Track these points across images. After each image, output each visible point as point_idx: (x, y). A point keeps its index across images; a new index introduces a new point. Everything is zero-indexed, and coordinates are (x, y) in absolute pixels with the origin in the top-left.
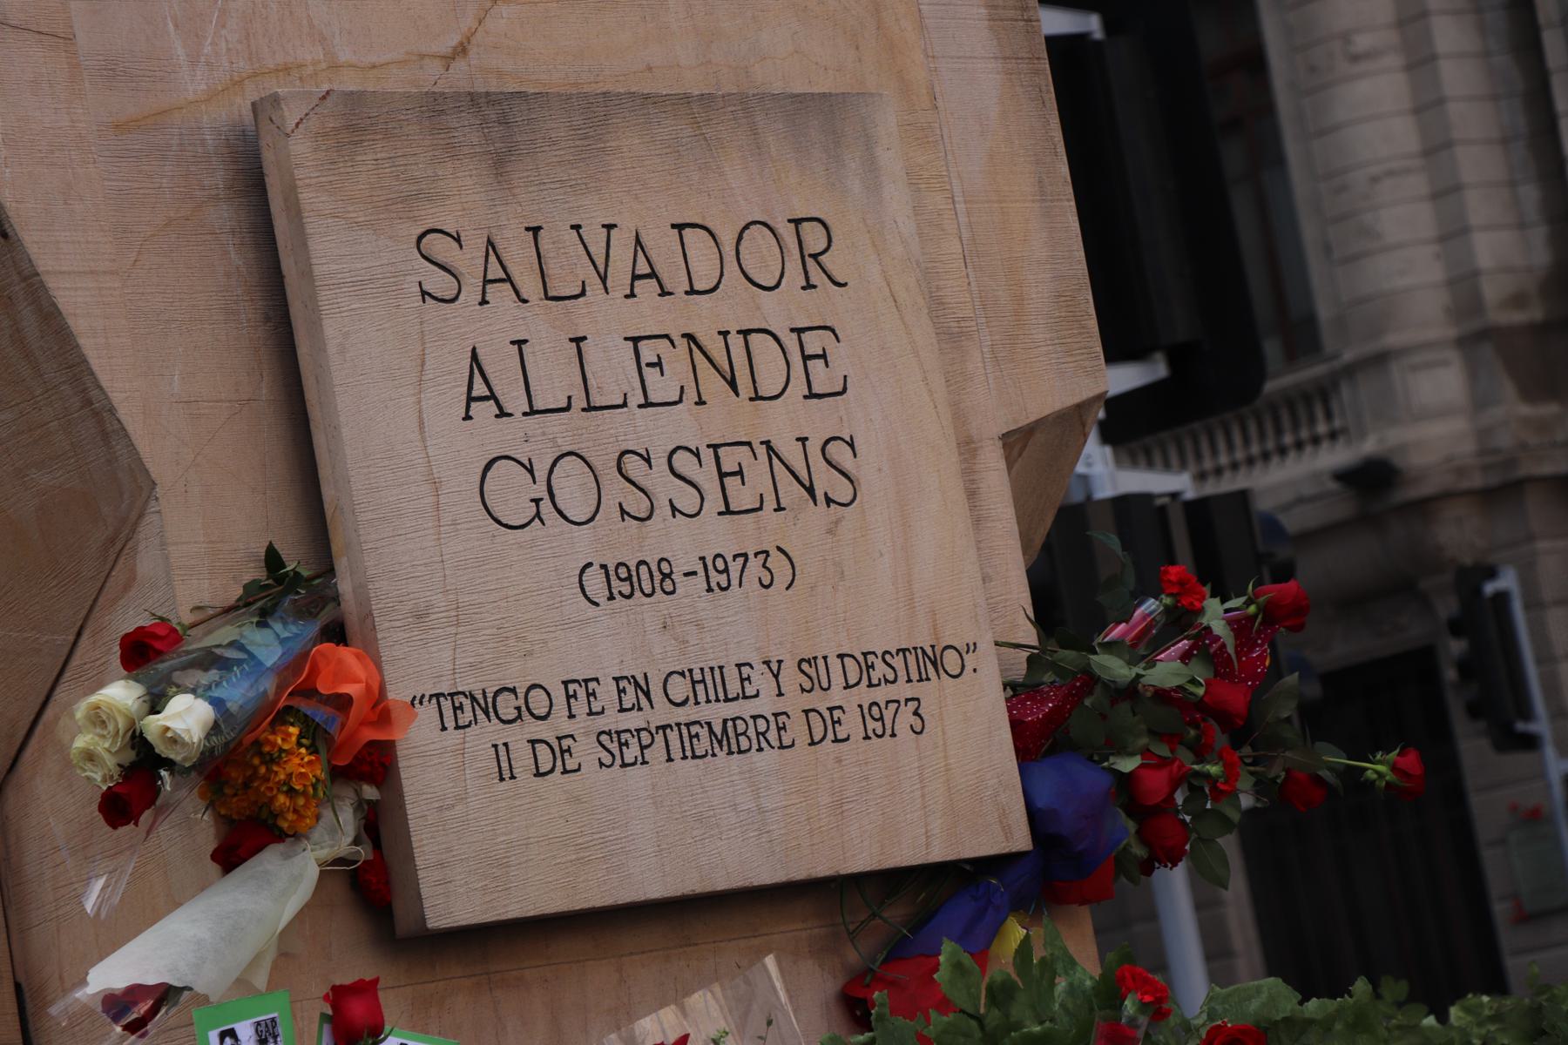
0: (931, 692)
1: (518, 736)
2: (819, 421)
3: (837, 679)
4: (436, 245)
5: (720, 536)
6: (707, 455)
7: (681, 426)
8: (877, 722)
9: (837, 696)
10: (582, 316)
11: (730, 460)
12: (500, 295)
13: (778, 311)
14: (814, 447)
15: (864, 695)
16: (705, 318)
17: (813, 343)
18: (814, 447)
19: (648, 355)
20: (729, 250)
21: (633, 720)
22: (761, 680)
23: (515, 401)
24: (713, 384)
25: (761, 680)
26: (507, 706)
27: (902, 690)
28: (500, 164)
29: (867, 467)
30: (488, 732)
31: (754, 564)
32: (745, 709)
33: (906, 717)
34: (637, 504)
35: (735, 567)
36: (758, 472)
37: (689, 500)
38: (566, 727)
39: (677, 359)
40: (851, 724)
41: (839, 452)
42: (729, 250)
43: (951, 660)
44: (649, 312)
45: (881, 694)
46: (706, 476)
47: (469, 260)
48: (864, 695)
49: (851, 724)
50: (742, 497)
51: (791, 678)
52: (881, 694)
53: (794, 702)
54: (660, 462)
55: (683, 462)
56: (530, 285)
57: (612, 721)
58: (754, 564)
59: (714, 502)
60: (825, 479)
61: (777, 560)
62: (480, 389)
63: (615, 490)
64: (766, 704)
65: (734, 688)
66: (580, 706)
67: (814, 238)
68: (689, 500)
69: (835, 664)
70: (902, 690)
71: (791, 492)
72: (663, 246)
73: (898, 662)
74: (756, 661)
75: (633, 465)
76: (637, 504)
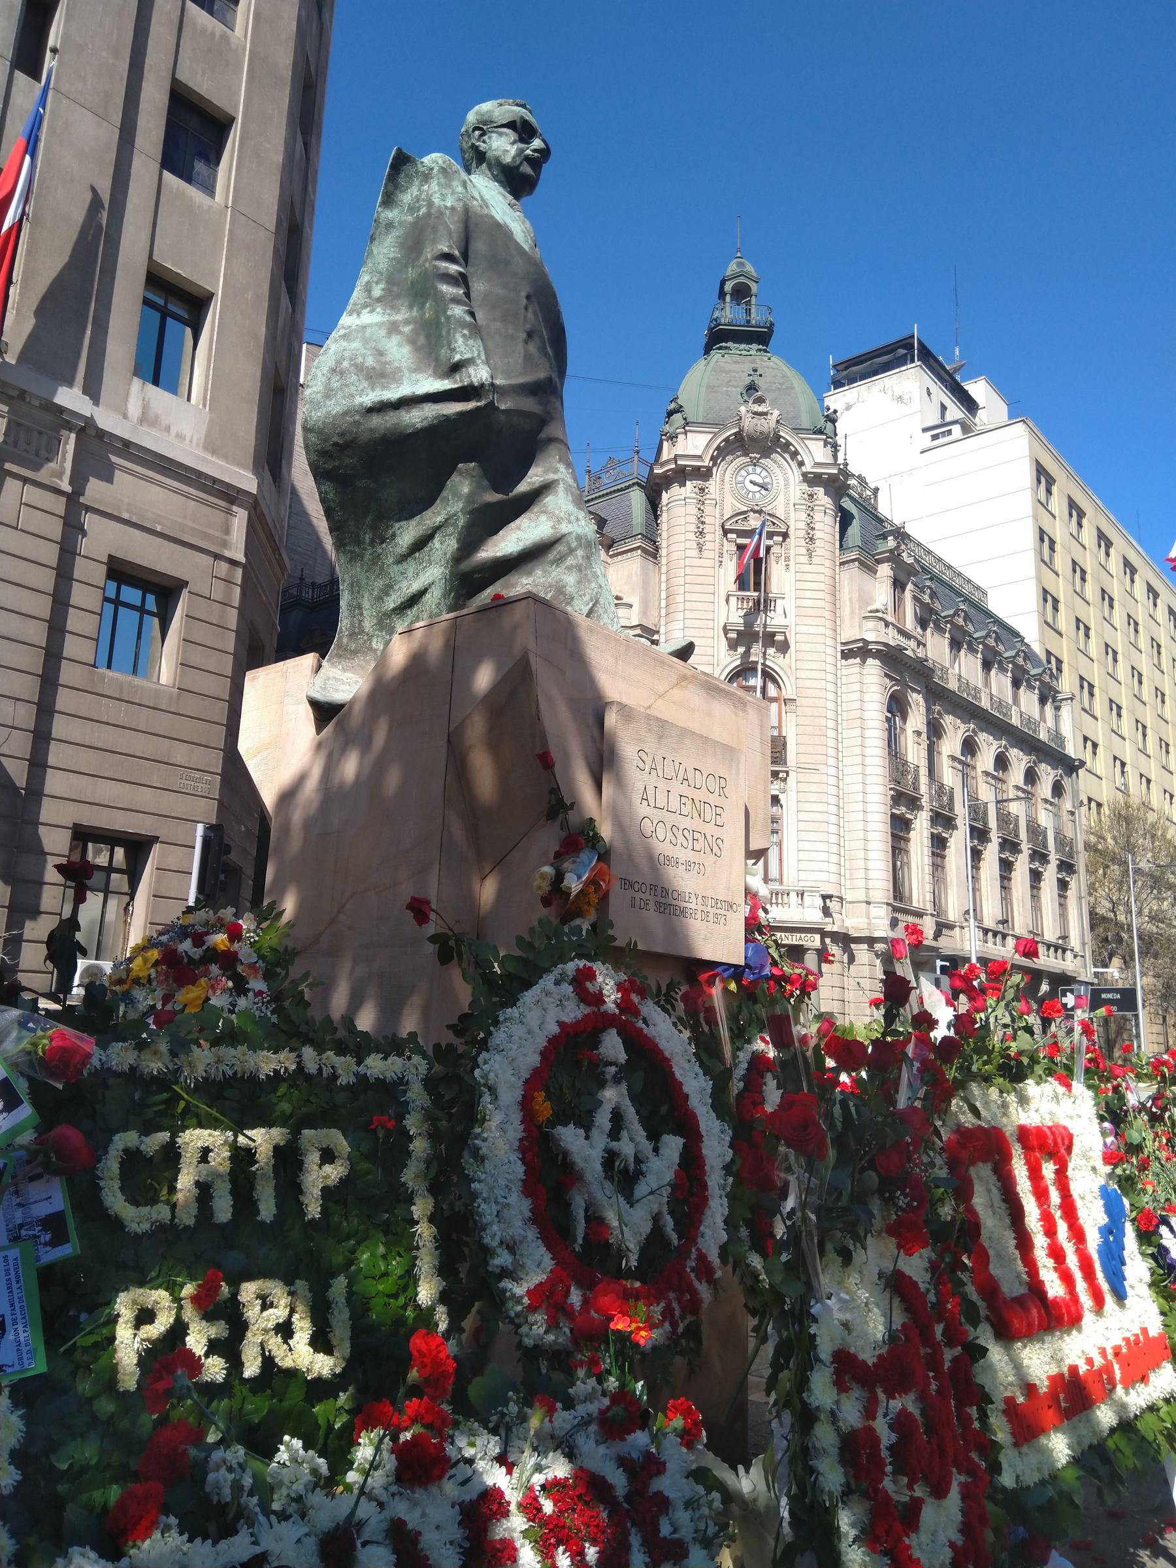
2: (717, 832)
11: (696, 835)
13: (713, 799)
16: (699, 795)
17: (719, 811)
23: (652, 804)
24: (696, 815)
26: (637, 886)
27: (723, 912)
33: (722, 921)
36: (701, 840)
38: (649, 897)
44: (684, 789)
45: (719, 911)
49: (711, 918)
52: (719, 911)
56: (661, 775)
59: (690, 846)
60: (715, 849)
63: (669, 834)
68: (685, 845)
70: (723, 912)
71: (708, 850)
72: (691, 772)
76: (674, 842)
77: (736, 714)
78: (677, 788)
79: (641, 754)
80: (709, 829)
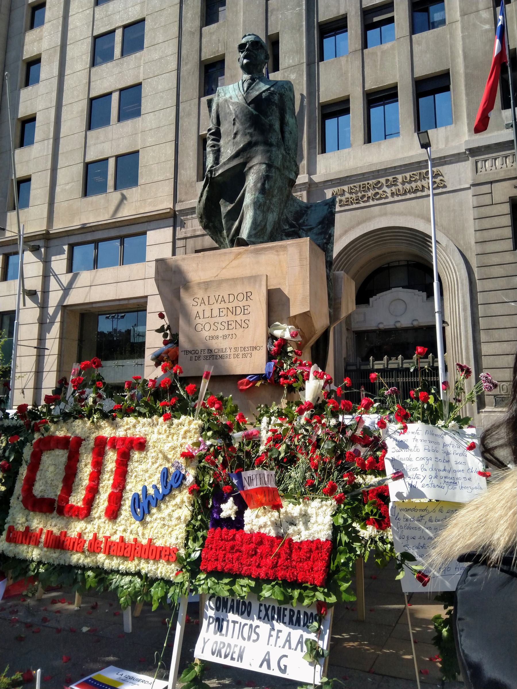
0: (254, 353)
1: (194, 356)
2: (244, 318)
3: (240, 350)
4: (196, 300)
5: (226, 332)
6: (227, 323)
7: (225, 319)
8: (244, 356)
9: (239, 352)
10: (213, 307)
12: (203, 305)
13: (241, 304)
14: (243, 321)
15: (243, 352)
16: (230, 306)
18: (243, 321)
19: (221, 310)
20: (236, 297)
21: (209, 354)
22: (228, 350)
24: (229, 312)
25: (228, 350)
26: (193, 352)
28: (206, 289)
29: (251, 324)
30: (190, 355)
31: (231, 336)
32: (225, 353)
33: (249, 355)
34: (215, 328)
35: (227, 336)
37: (223, 328)
39: (225, 311)
40: (240, 356)
41: (247, 322)
42: (236, 297)
43: (258, 348)
44: (223, 305)
45: (246, 352)
46: (226, 325)
47: (199, 301)
48: (243, 352)
49: (240, 356)
50: (230, 327)
51: (233, 350)
52: (246, 352)
53: (232, 353)
54: (220, 323)
55: (223, 323)
56: (207, 303)
57: (206, 354)
58: (231, 336)
59: (226, 328)
60: (244, 325)
61: (234, 336)
62: (198, 316)
63: (213, 327)
64: (228, 353)
65: (224, 351)
66: (202, 353)
67: (249, 294)
69: (240, 348)
72: (226, 298)
73: (249, 348)
74: (228, 348)
75: (216, 324)
76: (215, 328)
77: (278, 255)
78: (216, 307)
79: (196, 300)
80: (238, 318)
